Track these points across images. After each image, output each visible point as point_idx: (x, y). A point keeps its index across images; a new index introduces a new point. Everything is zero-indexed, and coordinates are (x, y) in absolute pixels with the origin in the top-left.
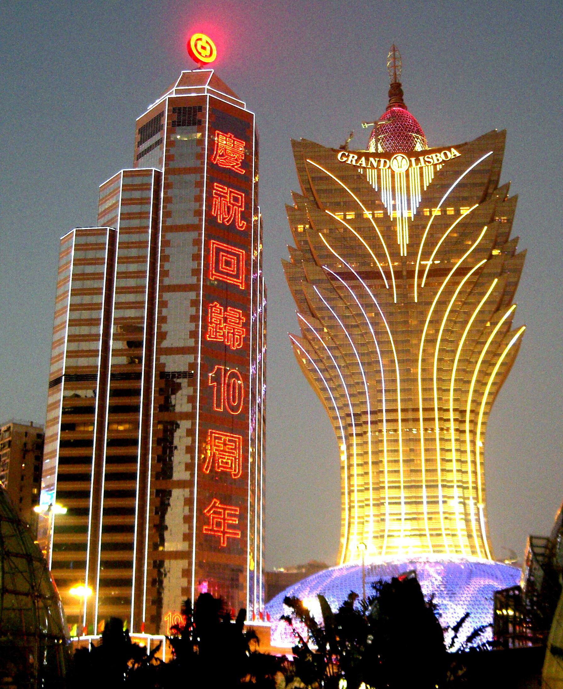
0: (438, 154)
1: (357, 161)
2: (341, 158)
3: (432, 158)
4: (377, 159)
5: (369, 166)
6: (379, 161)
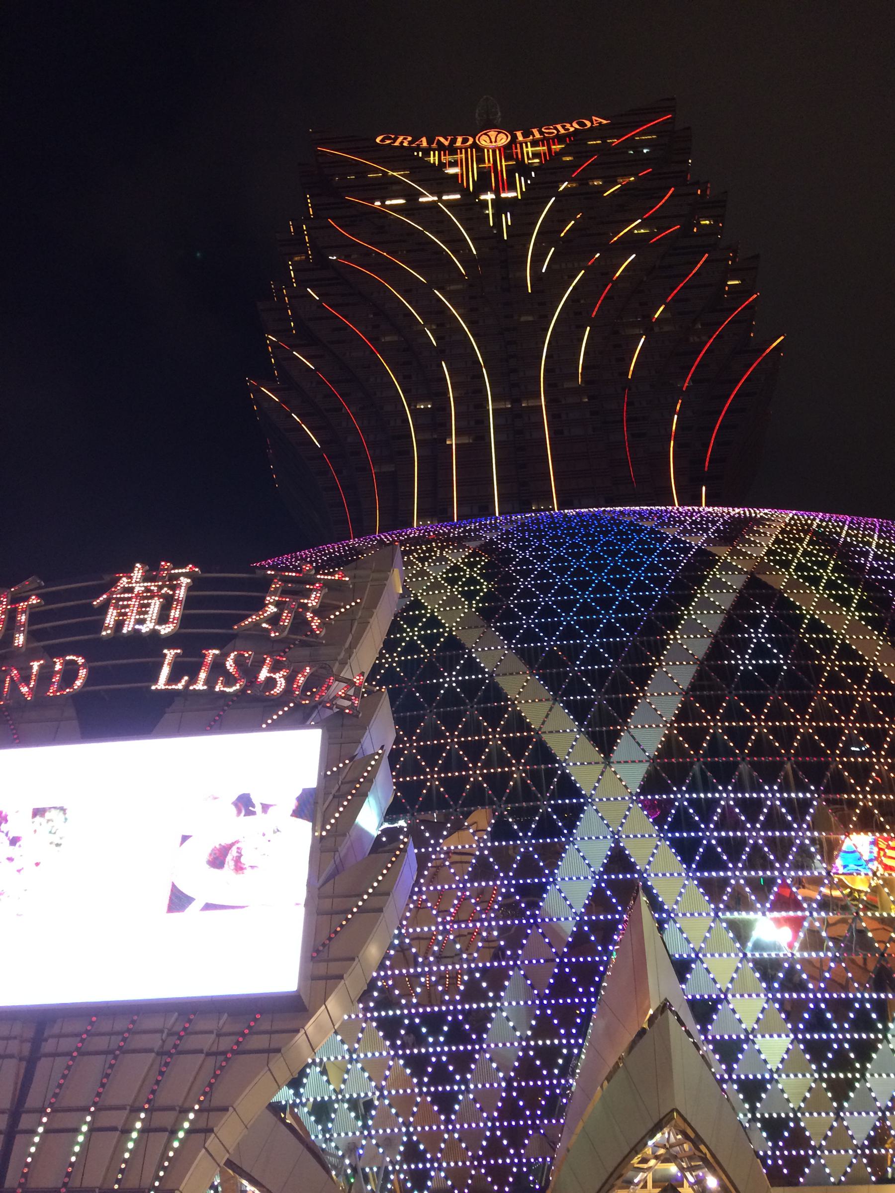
1: (410, 143)
2: (382, 141)
3: (556, 129)
4: (449, 138)
5: (434, 145)
6: (454, 141)
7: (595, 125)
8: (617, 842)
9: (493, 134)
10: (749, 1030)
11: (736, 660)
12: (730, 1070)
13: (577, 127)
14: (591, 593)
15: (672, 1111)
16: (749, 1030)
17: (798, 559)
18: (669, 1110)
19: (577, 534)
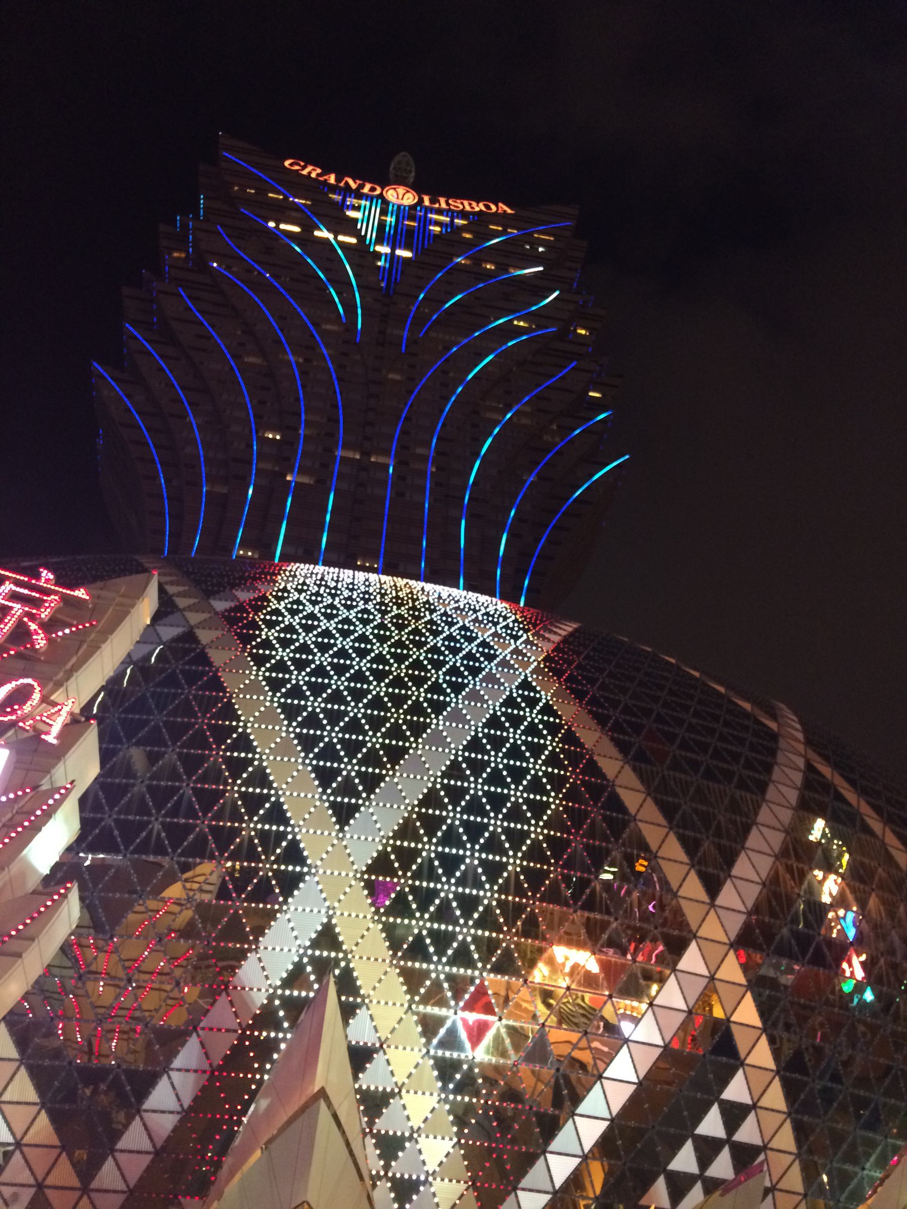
0: (474, 204)
1: (318, 175)
2: (291, 165)
3: (462, 204)
4: (358, 182)
5: (342, 184)
6: (362, 186)
7: (500, 211)
8: (330, 918)
9: (401, 190)
10: (415, 1128)
11: (490, 756)
12: (387, 1167)
13: (483, 209)
14: (368, 661)
15: (304, 1202)
16: (415, 1128)
17: (526, 676)
18: (299, 1202)
19: (371, 600)
